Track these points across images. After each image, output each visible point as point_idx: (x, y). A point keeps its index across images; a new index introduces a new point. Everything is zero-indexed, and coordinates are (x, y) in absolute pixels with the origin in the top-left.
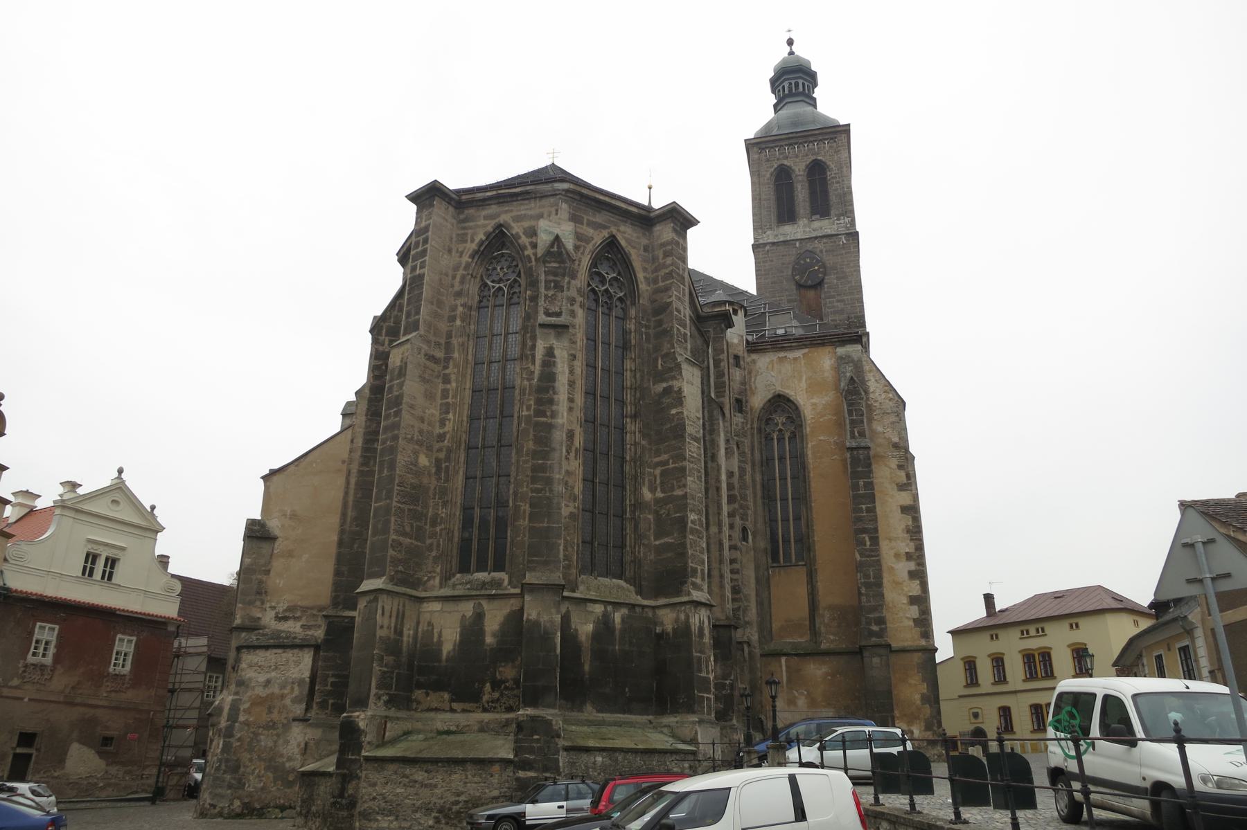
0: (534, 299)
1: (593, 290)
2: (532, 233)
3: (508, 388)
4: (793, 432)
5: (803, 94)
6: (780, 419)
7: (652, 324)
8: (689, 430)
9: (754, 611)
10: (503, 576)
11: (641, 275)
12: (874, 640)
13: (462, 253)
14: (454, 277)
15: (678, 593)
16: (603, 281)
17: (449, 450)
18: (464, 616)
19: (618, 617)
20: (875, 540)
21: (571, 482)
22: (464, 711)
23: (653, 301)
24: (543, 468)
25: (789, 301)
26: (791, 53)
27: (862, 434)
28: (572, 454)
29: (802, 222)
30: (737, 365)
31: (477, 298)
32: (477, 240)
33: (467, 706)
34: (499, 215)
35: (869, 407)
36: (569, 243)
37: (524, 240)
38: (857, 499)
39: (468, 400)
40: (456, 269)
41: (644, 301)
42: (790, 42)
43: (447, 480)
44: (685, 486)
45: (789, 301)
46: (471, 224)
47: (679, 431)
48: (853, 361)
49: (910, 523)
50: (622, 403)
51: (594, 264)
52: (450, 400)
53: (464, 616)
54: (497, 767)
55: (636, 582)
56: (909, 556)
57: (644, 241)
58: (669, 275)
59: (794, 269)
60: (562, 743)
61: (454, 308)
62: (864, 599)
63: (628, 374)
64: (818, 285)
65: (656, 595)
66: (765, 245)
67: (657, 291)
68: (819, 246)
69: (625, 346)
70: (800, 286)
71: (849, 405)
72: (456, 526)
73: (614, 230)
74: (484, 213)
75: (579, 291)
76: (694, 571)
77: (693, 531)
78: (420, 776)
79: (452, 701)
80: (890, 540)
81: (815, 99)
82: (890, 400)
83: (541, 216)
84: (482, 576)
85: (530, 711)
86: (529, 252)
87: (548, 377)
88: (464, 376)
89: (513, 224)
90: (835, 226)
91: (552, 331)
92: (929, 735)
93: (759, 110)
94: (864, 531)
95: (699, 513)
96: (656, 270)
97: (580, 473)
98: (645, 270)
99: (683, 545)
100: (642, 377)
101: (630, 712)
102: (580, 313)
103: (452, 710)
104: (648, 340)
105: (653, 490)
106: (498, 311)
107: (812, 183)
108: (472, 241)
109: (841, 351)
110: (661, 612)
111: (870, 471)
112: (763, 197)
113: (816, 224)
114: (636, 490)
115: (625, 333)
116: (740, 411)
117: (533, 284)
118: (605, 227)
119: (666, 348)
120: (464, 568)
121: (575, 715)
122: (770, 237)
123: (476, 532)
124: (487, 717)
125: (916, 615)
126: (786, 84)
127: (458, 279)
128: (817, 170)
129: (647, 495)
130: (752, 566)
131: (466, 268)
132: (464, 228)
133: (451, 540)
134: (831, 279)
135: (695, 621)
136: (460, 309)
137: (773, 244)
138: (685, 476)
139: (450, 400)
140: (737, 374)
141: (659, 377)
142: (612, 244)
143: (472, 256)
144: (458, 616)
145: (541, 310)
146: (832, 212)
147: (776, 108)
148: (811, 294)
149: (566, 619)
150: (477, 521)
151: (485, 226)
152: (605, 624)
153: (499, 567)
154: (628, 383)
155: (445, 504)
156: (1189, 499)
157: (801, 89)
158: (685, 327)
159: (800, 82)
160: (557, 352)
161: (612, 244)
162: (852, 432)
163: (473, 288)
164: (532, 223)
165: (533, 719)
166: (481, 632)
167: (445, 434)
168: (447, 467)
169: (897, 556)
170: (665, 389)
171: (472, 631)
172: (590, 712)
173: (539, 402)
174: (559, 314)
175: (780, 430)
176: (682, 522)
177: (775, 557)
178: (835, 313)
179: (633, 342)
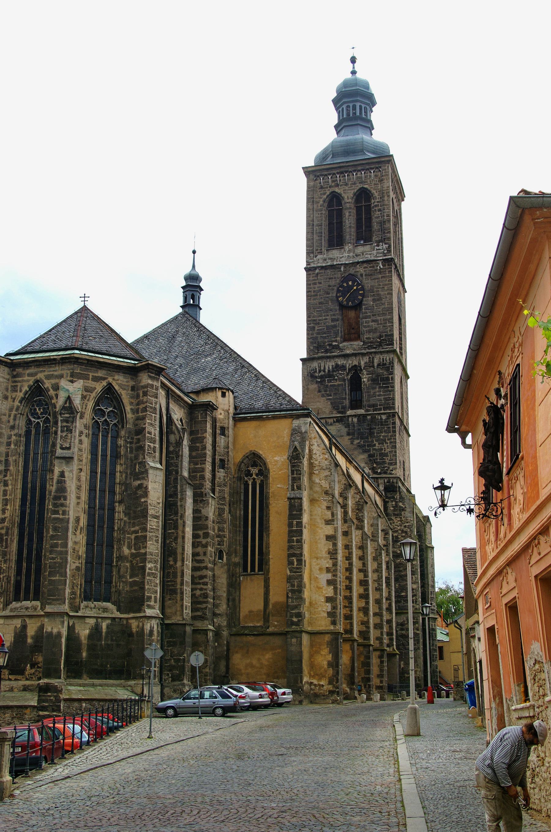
1: (96, 421)
2: (56, 388)
4: (262, 481)
6: (254, 471)
7: (135, 441)
8: (151, 512)
9: (225, 606)
10: (38, 603)
11: (128, 408)
13: (14, 399)
14: (10, 416)
15: (139, 610)
16: (103, 413)
17: (8, 529)
18: (16, 627)
19: (104, 625)
20: (300, 561)
21: (77, 548)
22: (16, 680)
23: (136, 425)
25: (333, 320)
26: (354, 73)
27: (299, 488)
28: (79, 531)
30: (223, 433)
31: (24, 429)
32: (24, 391)
33: (19, 677)
34: (36, 374)
35: (311, 465)
37: (52, 392)
38: (291, 533)
39: (19, 496)
40: (11, 410)
42: (353, 60)
43: (6, 547)
44: (146, 547)
45: (333, 320)
46: (20, 379)
47: (144, 514)
48: (301, 433)
49: (331, 547)
50: (112, 492)
51: (97, 404)
52: (8, 497)
53: (16, 627)
54: (28, 711)
56: (328, 570)
57: (132, 383)
59: (338, 291)
61: (10, 437)
62: (290, 600)
63: (118, 474)
64: (358, 306)
66: (315, 268)
67: (138, 419)
68: (360, 270)
69: (116, 456)
70: (342, 307)
72: (13, 573)
73: (110, 380)
74: (28, 372)
75: (85, 426)
76: (149, 598)
77: (149, 574)
79: (10, 674)
80: (317, 558)
81: (370, 122)
82: (326, 459)
83: (61, 376)
85: (46, 681)
88: (16, 480)
89: (45, 381)
91: (63, 461)
92: (331, 687)
93: (320, 132)
95: (156, 562)
96: (138, 404)
98: (131, 403)
99: (143, 583)
100: (126, 477)
101: (110, 679)
103: (10, 680)
104: (131, 452)
105: (129, 548)
107: (359, 210)
108: (21, 391)
109: (296, 423)
110: (131, 621)
111: (301, 515)
113: (360, 249)
114: (119, 549)
115: (117, 446)
116: (223, 468)
117: (56, 423)
118: (104, 379)
119: (141, 457)
120: (17, 599)
122: (320, 261)
123: (24, 577)
124: (28, 683)
125: (329, 610)
126: (344, 106)
127: (12, 417)
128: (363, 196)
129: (126, 551)
130: (225, 576)
131: (17, 409)
132: (16, 382)
133: (9, 582)
134: (369, 301)
135: (147, 627)
136: (14, 437)
137: (322, 268)
138: (146, 541)
139: (8, 497)
140: (221, 441)
142: (109, 389)
143: (21, 402)
144: (13, 627)
145: (58, 446)
146: (374, 238)
147: (338, 128)
148: (352, 314)
149: (71, 629)
150: (24, 571)
151: (28, 381)
152: (96, 631)
153: (36, 598)
154: (118, 481)
155: (5, 562)
156: (468, 547)
158: (154, 442)
159: (358, 104)
160: (66, 474)
161: (109, 389)
162: (293, 486)
163: (22, 423)
164: (57, 381)
165: (47, 684)
166: (26, 636)
167: (5, 518)
168: (7, 539)
169: (321, 569)
170: (139, 484)
171: (20, 635)
174: (69, 448)
175: (254, 479)
176: (144, 568)
177: (245, 569)
178: (369, 332)
179: (122, 453)
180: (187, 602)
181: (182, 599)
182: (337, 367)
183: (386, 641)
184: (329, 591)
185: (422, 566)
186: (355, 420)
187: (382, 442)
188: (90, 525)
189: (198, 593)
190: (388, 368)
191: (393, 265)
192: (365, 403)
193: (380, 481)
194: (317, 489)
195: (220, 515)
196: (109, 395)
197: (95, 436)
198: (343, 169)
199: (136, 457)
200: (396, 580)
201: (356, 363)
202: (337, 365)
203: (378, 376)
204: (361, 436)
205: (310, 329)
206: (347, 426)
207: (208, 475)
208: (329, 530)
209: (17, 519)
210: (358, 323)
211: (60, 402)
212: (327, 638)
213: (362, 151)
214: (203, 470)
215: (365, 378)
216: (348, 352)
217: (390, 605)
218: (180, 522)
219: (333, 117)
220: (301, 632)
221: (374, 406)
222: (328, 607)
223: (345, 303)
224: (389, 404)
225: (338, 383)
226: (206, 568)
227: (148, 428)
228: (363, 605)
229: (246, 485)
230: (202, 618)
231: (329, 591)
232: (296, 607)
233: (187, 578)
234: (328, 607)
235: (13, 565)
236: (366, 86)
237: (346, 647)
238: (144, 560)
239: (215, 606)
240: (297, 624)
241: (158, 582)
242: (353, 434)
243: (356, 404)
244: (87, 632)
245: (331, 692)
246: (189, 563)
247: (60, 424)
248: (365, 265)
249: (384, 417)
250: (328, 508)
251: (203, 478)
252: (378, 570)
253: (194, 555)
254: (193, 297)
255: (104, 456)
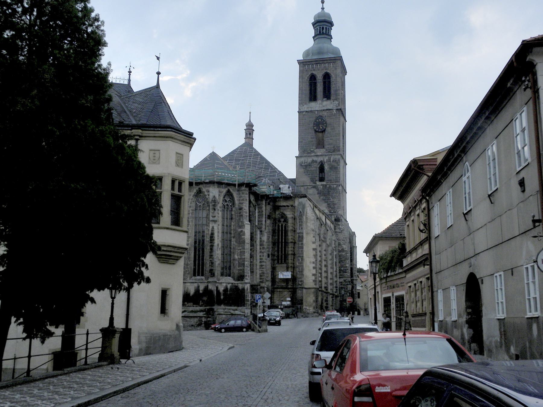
0: (209, 210)
3: (203, 232)
5: (326, 34)
6: (282, 220)
10: (203, 277)
11: (236, 199)
12: (300, 286)
15: (242, 280)
19: (229, 286)
20: (302, 259)
24: (212, 256)
25: (311, 138)
26: (323, 9)
27: (302, 229)
29: (319, 102)
35: (307, 218)
36: (217, 196)
37: (206, 193)
41: (237, 206)
45: (311, 138)
47: (244, 242)
55: (233, 278)
56: (313, 263)
58: (243, 200)
59: (314, 124)
60: (217, 313)
61: (189, 211)
63: (232, 226)
64: (323, 131)
65: (239, 280)
66: (303, 112)
67: (240, 203)
68: (325, 114)
70: (316, 131)
71: (300, 219)
75: (220, 207)
77: (247, 266)
78: (188, 319)
84: (198, 277)
86: (207, 197)
87: (212, 234)
90: (332, 105)
92: (314, 311)
94: (300, 257)
97: (220, 254)
102: (220, 213)
106: (201, 211)
107: (324, 83)
112: (304, 89)
114: (234, 256)
115: (232, 215)
117: (209, 206)
120: (194, 275)
121: (219, 307)
122: (305, 108)
126: (318, 27)
128: (327, 77)
129: (236, 257)
134: (328, 129)
136: (191, 211)
141: (240, 227)
142: (229, 191)
146: (332, 98)
148: (320, 134)
153: (202, 275)
157: (324, 31)
159: (325, 27)
163: (193, 205)
169: (310, 262)
171: (197, 290)
172: (223, 306)
173: (211, 240)
176: (244, 264)
177: (278, 262)
178: (329, 144)
180: (258, 276)
181: (256, 275)
182: (313, 161)
183: (335, 290)
184: (314, 272)
185: (351, 255)
186: (321, 187)
187: (334, 198)
188: (223, 247)
189: (261, 272)
190: (337, 162)
191: (341, 112)
192: (326, 179)
193: (333, 216)
194: (309, 228)
195: (268, 239)
196: (229, 193)
197: (223, 211)
198: (318, 62)
199: (239, 219)
200: (339, 262)
201: (322, 159)
202: (313, 160)
203: (332, 166)
204: (324, 195)
205: (300, 142)
206: (318, 190)
207: (264, 223)
208: (314, 246)
209: (193, 244)
210: (323, 139)
211: (211, 198)
212: (313, 290)
213: (327, 53)
214: (262, 221)
215: (326, 167)
216: (318, 154)
217: (336, 274)
218: (255, 244)
219: (312, 32)
220: (302, 288)
221: (330, 180)
222: (313, 278)
223: (317, 130)
224: (337, 180)
225: (314, 169)
226: (264, 262)
227: (244, 207)
228: (326, 275)
229: (279, 226)
230: (262, 282)
231: (314, 272)
232: (301, 278)
233: (258, 267)
234: (313, 278)
235: (192, 262)
236: (329, 16)
237: (320, 293)
238: (244, 261)
239: (267, 277)
240: (301, 285)
241: (249, 269)
242: (320, 194)
243: (322, 179)
244: (223, 289)
245: (315, 312)
246: (259, 261)
247: (211, 207)
248: (327, 111)
249: (335, 186)
250: (314, 237)
251: (262, 224)
252: (332, 259)
253: (260, 256)
254: (250, 134)
255: (227, 218)
